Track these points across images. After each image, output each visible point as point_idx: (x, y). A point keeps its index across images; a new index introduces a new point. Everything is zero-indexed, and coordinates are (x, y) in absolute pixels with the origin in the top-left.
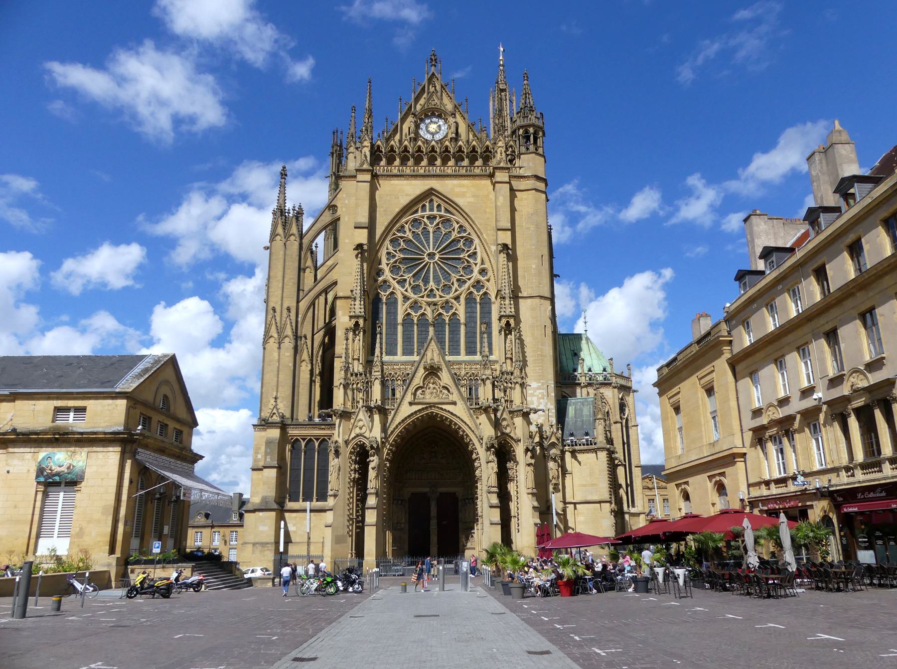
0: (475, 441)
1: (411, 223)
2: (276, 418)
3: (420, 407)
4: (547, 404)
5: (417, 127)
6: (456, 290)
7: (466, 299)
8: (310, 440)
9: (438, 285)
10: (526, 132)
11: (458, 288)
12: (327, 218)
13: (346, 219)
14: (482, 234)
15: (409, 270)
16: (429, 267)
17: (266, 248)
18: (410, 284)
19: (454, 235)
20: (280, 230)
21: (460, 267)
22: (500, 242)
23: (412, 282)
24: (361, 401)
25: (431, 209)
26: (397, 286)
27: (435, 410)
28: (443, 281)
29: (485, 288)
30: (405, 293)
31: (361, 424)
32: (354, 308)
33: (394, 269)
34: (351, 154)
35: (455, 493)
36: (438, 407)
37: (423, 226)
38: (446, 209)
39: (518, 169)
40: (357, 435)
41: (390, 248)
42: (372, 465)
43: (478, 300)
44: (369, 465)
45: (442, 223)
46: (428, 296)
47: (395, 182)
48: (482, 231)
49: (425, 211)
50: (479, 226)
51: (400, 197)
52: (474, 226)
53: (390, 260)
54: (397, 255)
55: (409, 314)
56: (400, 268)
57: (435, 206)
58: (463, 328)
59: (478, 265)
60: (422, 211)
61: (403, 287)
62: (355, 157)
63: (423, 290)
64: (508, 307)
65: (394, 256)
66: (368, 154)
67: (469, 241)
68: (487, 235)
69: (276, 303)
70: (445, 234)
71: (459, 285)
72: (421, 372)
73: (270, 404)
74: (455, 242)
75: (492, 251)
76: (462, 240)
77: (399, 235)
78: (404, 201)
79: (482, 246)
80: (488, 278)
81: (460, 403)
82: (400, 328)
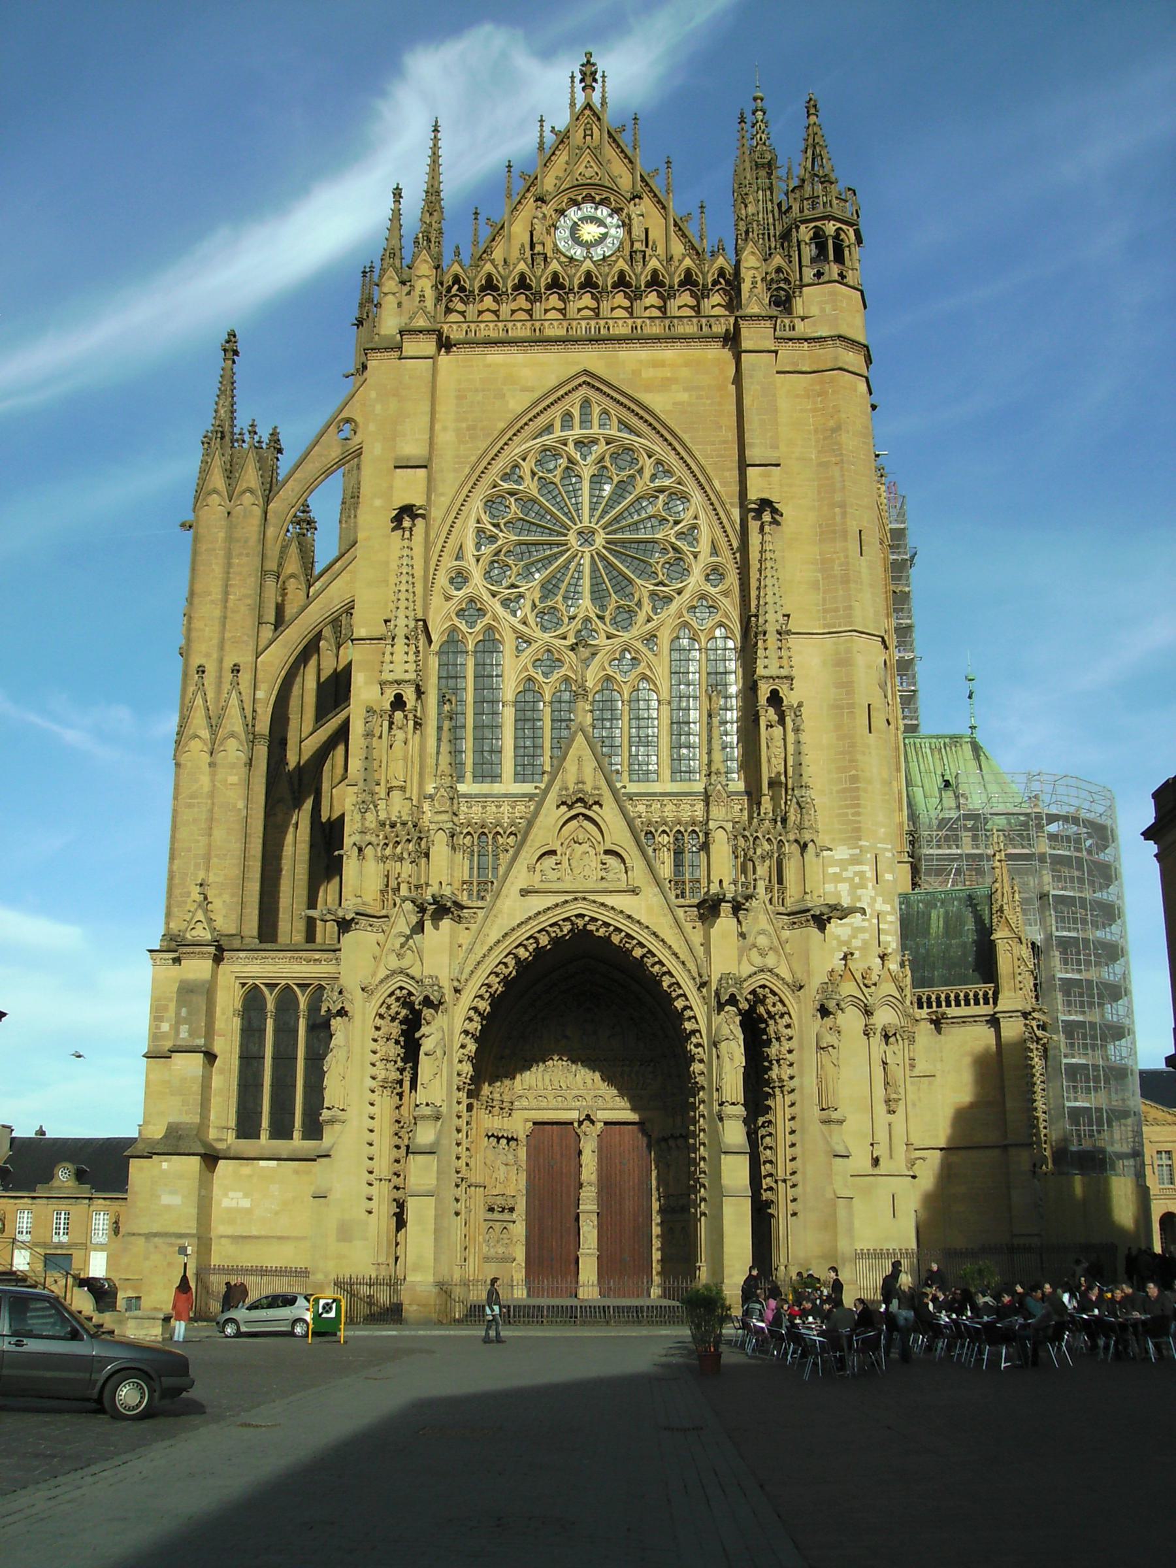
0: (689, 987)
2: (202, 933)
3: (551, 900)
4: (873, 899)
6: (649, 621)
12: (332, 450)
14: (709, 480)
18: (534, 606)
19: (642, 485)
20: (218, 480)
26: (500, 610)
27: (589, 911)
28: (613, 595)
34: (390, 297)
36: (594, 902)
38: (620, 421)
39: (797, 321)
40: (394, 973)
41: (485, 518)
47: (497, 357)
48: (709, 470)
50: (703, 462)
52: (689, 461)
55: (530, 679)
59: (701, 557)
62: (400, 305)
63: (566, 620)
66: (430, 294)
68: (724, 484)
69: (208, 655)
73: (189, 900)
76: (661, 497)
77: (506, 485)
78: (517, 403)
80: (725, 587)
82: (508, 715)
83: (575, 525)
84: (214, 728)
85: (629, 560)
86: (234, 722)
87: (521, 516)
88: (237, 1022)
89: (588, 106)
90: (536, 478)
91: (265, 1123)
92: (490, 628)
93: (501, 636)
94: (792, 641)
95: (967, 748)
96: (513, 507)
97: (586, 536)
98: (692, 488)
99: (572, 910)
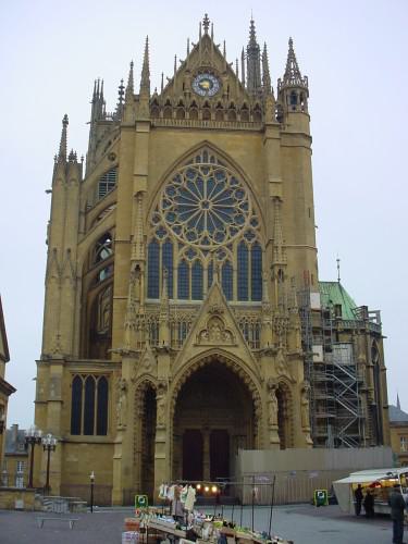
0: (256, 381)
3: (204, 349)
5: (191, 83)
8: (90, 378)
9: (212, 233)
10: (293, 93)
15: (183, 218)
17: (48, 192)
19: (227, 186)
20: (61, 175)
21: (233, 216)
24: (147, 343)
25: (206, 160)
31: (147, 364)
33: (171, 216)
35: (226, 430)
42: (159, 404)
44: (155, 402)
46: (203, 243)
47: (172, 133)
57: (209, 157)
58: (235, 275)
62: (134, 109)
66: (147, 107)
67: (241, 193)
72: (206, 317)
78: (180, 151)
81: (241, 345)
84: (60, 273)
86: (69, 272)
88: (71, 390)
89: (206, 35)
91: (82, 429)
92: (169, 239)
94: (286, 251)
95: (337, 287)
97: (205, 205)
98: (245, 188)
99: (212, 353)
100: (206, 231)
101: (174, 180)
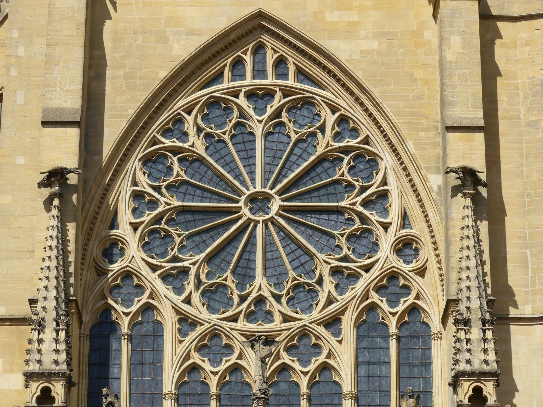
1: (201, 110)
7: (358, 325)
9: (279, 285)
11: (334, 293)
13: (20, 99)
14: (402, 141)
16: (253, 235)
18: (199, 282)
22: (454, 164)
23: (203, 277)
25: (259, 73)
29: (413, 294)
30: (185, 307)
32: (39, 351)
37: (235, 117)
43: (393, 329)
45: (288, 111)
46: (250, 316)
48: (404, 133)
49: (242, 77)
50: (394, 119)
51: (171, 38)
53: (141, 215)
54: (162, 199)
55: (195, 368)
56: (169, 236)
59: (392, 229)
60: (233, 78)
61: (179, 291)
63: (236, 299)
64: (477, 347)
65: (154, 204)
68: (418, 144)
70: (298, 141)
71: (337, 287)
74: (326, 165)
75: (429, 191)
76: (347, 159)
77: (168, 143)
79: (403, 174)
80: (419, 264)
83: (248, 190)
85: (310, 231)
87: (186, 178)
90: (203, 134)
93: (163, 317)
96: (176, 168)
100: (260, 280)
101: (166, 132)
